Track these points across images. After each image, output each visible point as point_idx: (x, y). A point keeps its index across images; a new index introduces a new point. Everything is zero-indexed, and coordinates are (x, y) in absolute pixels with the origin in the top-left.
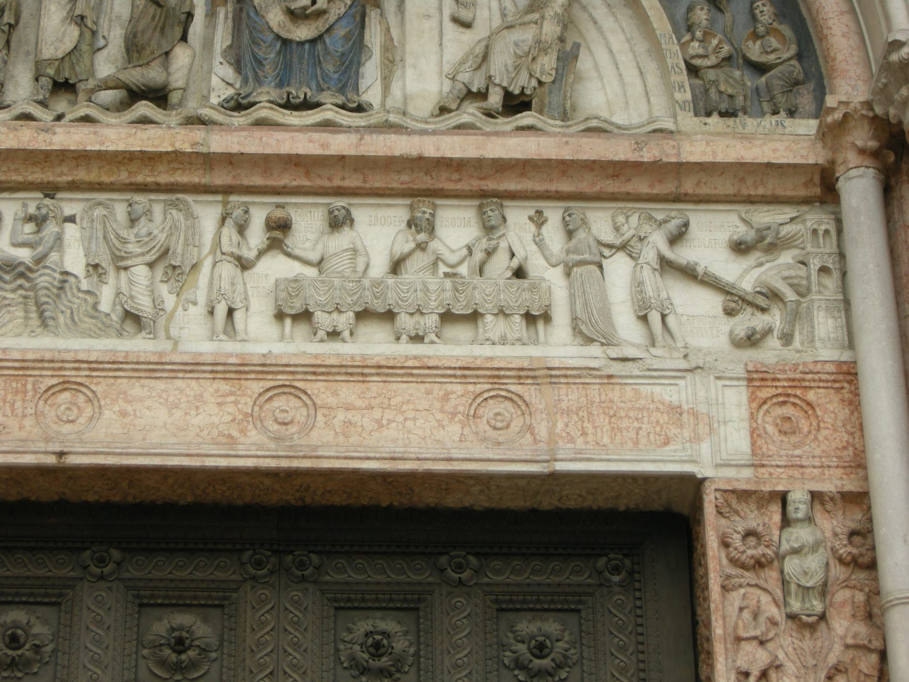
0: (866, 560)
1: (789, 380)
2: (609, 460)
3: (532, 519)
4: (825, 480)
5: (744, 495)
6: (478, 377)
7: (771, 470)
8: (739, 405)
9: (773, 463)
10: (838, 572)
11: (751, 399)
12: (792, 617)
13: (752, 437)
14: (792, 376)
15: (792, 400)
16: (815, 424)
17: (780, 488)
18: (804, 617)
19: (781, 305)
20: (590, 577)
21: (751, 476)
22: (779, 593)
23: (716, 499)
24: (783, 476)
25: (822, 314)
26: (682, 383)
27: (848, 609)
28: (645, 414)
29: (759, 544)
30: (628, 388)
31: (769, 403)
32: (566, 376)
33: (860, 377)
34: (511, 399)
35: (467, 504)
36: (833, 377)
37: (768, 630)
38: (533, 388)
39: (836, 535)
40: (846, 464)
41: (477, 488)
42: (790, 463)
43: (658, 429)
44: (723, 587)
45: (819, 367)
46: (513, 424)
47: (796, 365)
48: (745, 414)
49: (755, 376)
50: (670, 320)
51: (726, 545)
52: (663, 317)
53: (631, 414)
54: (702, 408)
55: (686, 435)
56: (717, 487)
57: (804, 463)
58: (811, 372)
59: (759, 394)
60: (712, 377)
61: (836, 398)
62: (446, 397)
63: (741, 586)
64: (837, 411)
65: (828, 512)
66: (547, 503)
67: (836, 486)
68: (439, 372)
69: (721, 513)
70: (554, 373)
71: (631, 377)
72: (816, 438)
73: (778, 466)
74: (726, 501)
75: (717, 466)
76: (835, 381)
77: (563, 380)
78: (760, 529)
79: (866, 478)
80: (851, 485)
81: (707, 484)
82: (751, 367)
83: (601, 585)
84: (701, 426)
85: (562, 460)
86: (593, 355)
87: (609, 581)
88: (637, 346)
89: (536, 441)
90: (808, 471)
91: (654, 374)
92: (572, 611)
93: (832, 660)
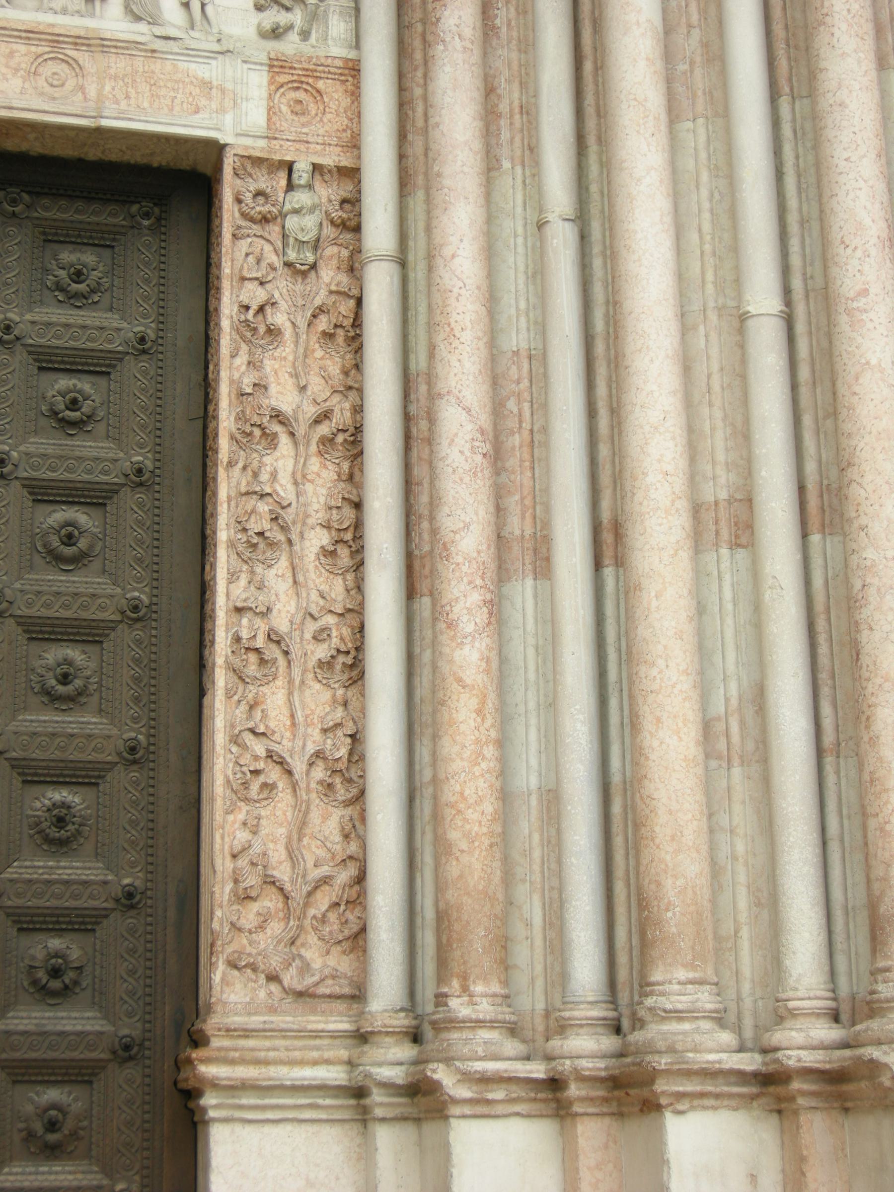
0: (353, 223)
1: (304, 69)
2: (147, 122)
3: (80, 165)
5: (258, 161)
6: (40, 40)
7: (282, 142)
8: (260, 86)
10: (329, 231)
11: (271, 82)
12: (288, 265)
13: (268, 114)
14: (306, 66)
15: (304, 86)
16: (321, 108)
17: (288, 158)
19: (302, 6)
20: (124, 219)
22: (279, 244)
25: (336, 17)
26: (214, 62)
27: (335, 262)
28: (181, 85)
29: (266, 203)
30: (168, 63)
31: (285, 87)
32: (116, 47)
33: (362, 73)
34: (67, 62)
35: (24, 149)
37: (268, 274)
38: (87, 54)
39: (330, 201)
41: (32, 136)
43: (191, 99)
45: (329, 61)
46: (67, 84)
47: (311, 58)
48: (265, 94)
49: (276, 63)
50: (209, 9)
51: (239, 201)
52: (203, 5)
53: (169, 85)
54: (229, 86)
55: (214, 106)
57: (310, 140)
58: (322, 65)
59: (277, 78)
60: (239, 61)
61: (341, 89)
62: (11, 54)
63: (248, 236)
66: (92, 155)
68: (7, 32)
70: (106, 43)
71: (171, 53)
72: (321, 120)
75: (238, 135)
76: (341, 74)
77: (113, 50)
78: (269, 190)
79: (359, 157)
80: (346, 162)
81: (228, 149)
82: (272, 56)
83: (133, 227)
84: (227, 100)
85: (107, 118)
86: (141, 31)
88: (179, 28)
89: (86, 99)
90: (312, 146)
91: (191, 53)
92: (108, 246)
93: (318, 302)
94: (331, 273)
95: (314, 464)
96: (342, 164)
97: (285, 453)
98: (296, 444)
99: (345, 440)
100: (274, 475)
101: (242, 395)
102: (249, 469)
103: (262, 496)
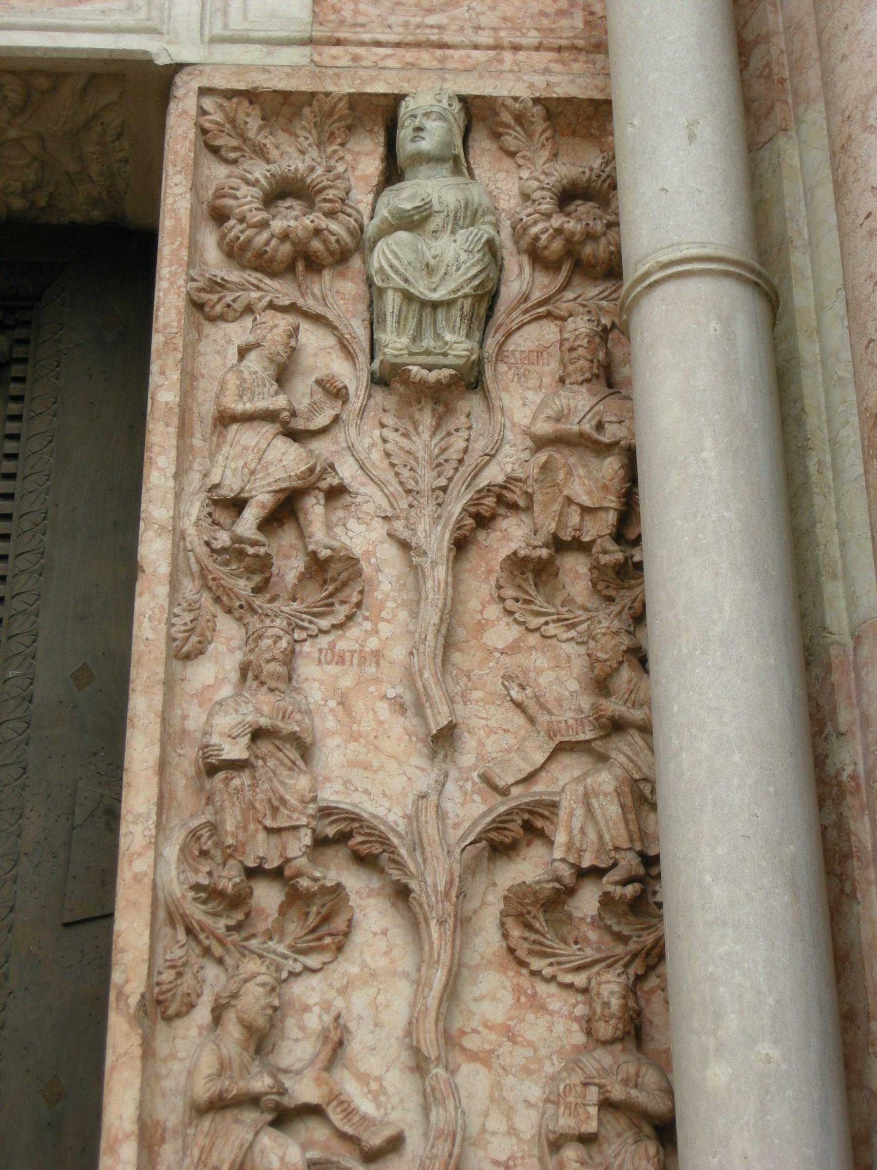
5: (282, 107)
7: (360, 51)
9: (366, 37)
12: (383, 379)
17: (379, 88)
18: (414, 369)
21: (305, 61)
23: (203, 112)
24: (389, 63)
37: (315, 409)
40: (564, 42)
42: (410, 38)
44: (197, 305)
56: (206, 83)
65: (512, 154)
67: (531, 86)
69: (215, 151)
73: (378, 44)
74: (232, 121)
75: (213, 40)
80: (569, 83)
81: (180, 79)
93: (494, 475)
94: (535, 398)
95: (492, 995)
96: (560, 92)
97: (380, 963)
98: (416, 926)
99: (606, 901)
100: (336, 1046)
101: (212, 770)
102: (230, 1018)
103: (285, 1117)
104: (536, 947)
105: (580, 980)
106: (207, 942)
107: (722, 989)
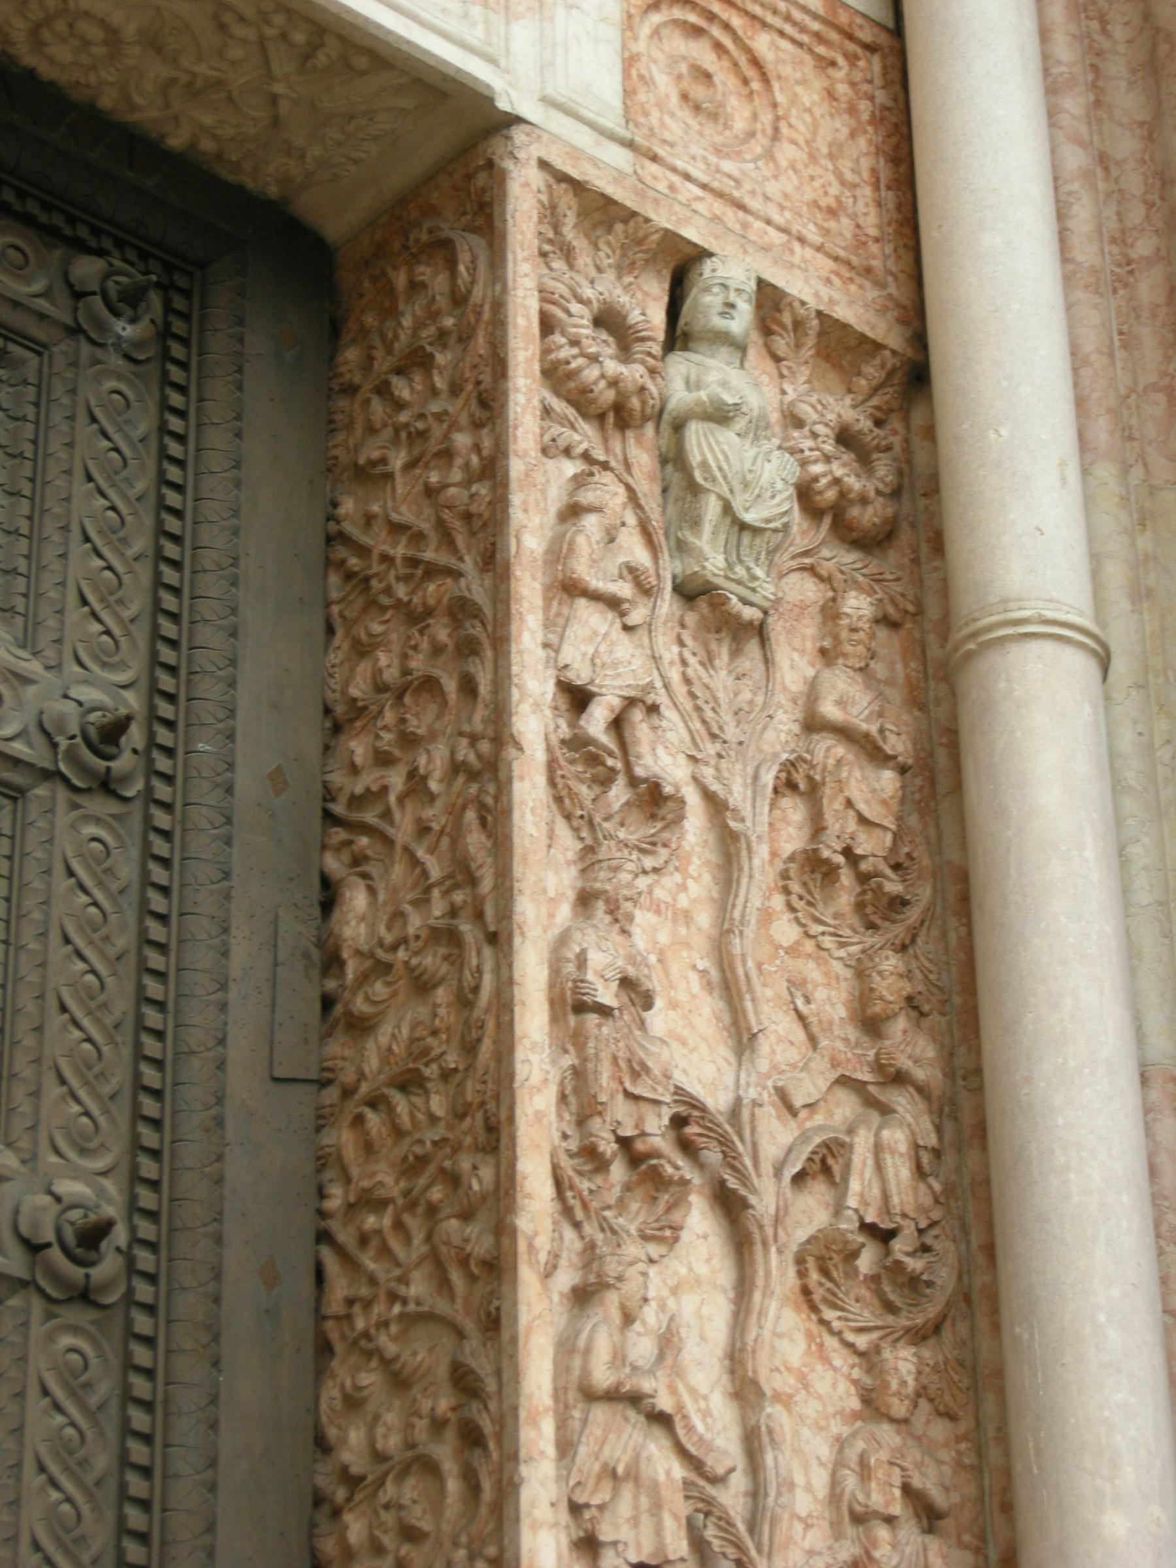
4: (792, 266)
12: (691, 592)
13: (626, 75)
15: (716, 32)
16: (766, 118)
17: (691, 233)
18: (734, 599)
21: (629, 170)
24: (700, 207)
36: (816, 26)
64: (818, 112)
65: (777, 359)
72: (769, 155)
75: (548, 102)
76: (818, 36)
81: (518, 134)
83: (75, 331)
87: (103, 328)
97: (703, 1270)
101: (580, 1008)
104: (830, 1297)
105: (862, 1342)
106: (572, 1202)
107: (1119, 1438)
